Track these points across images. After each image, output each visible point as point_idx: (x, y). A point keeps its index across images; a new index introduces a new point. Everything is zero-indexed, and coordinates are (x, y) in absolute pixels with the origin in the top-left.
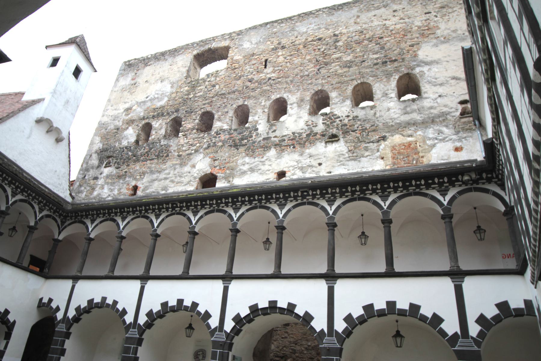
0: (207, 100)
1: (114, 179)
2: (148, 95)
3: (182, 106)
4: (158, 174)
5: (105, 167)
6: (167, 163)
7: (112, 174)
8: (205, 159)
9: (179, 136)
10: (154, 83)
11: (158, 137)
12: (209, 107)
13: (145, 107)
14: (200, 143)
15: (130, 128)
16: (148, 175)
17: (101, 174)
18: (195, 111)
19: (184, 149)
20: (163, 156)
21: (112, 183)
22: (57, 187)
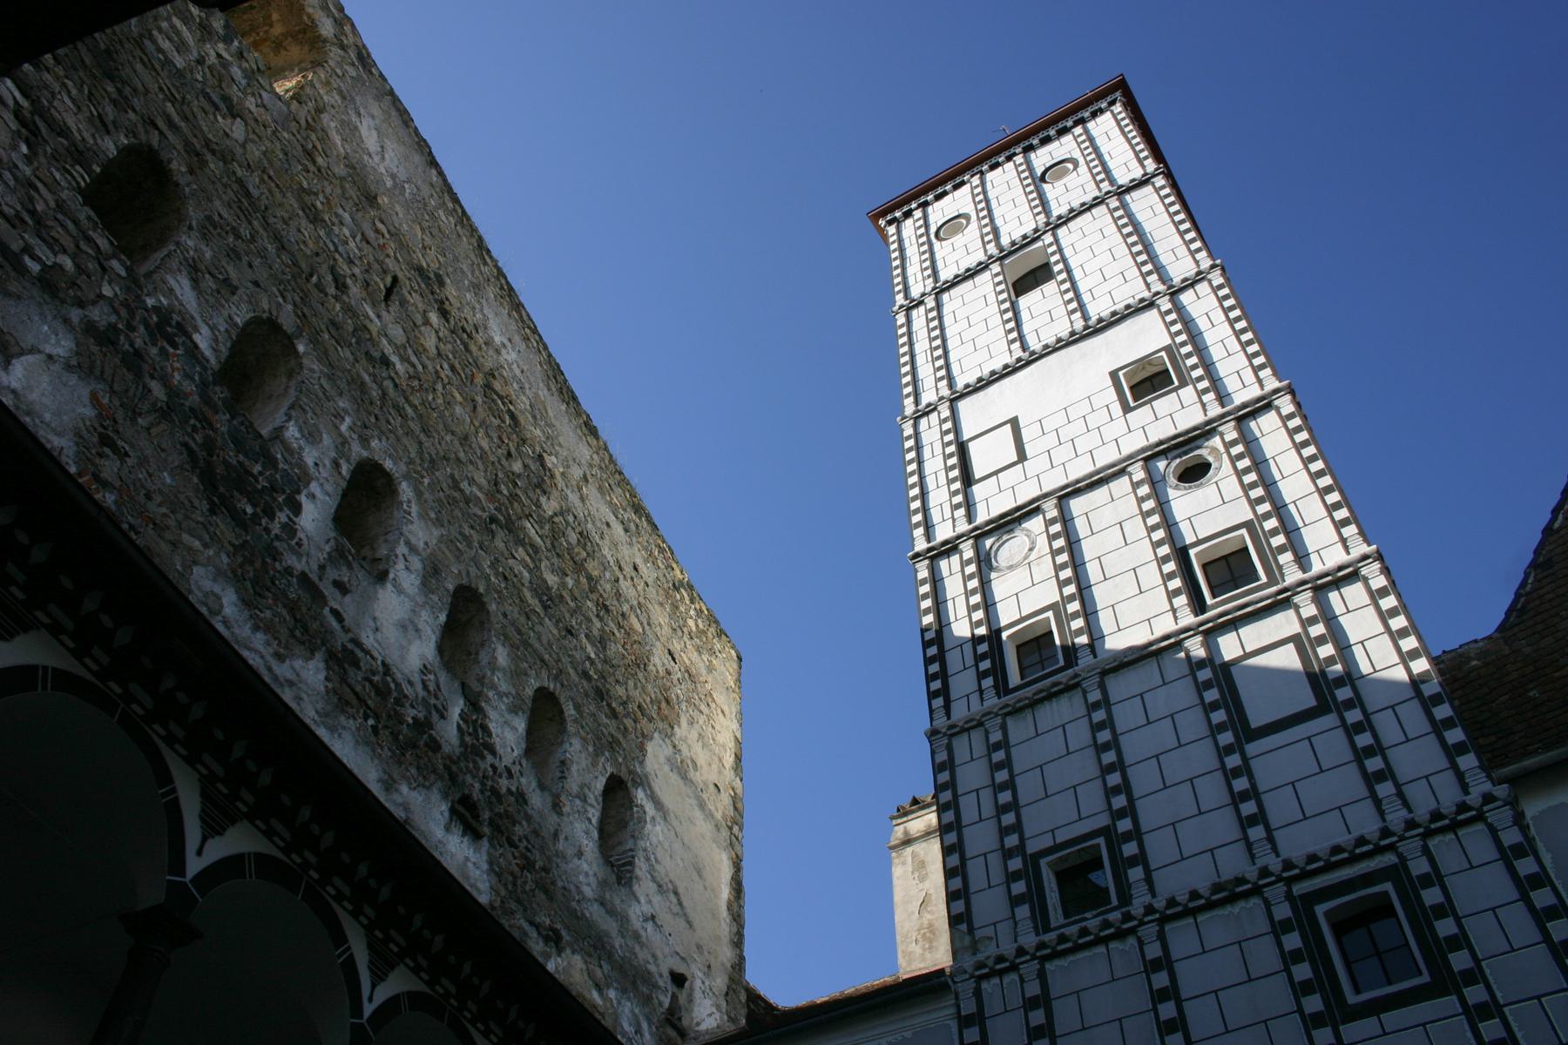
0: (186, 119)
8: (73, 380)
12: (183, 169)
18: (127, 91)
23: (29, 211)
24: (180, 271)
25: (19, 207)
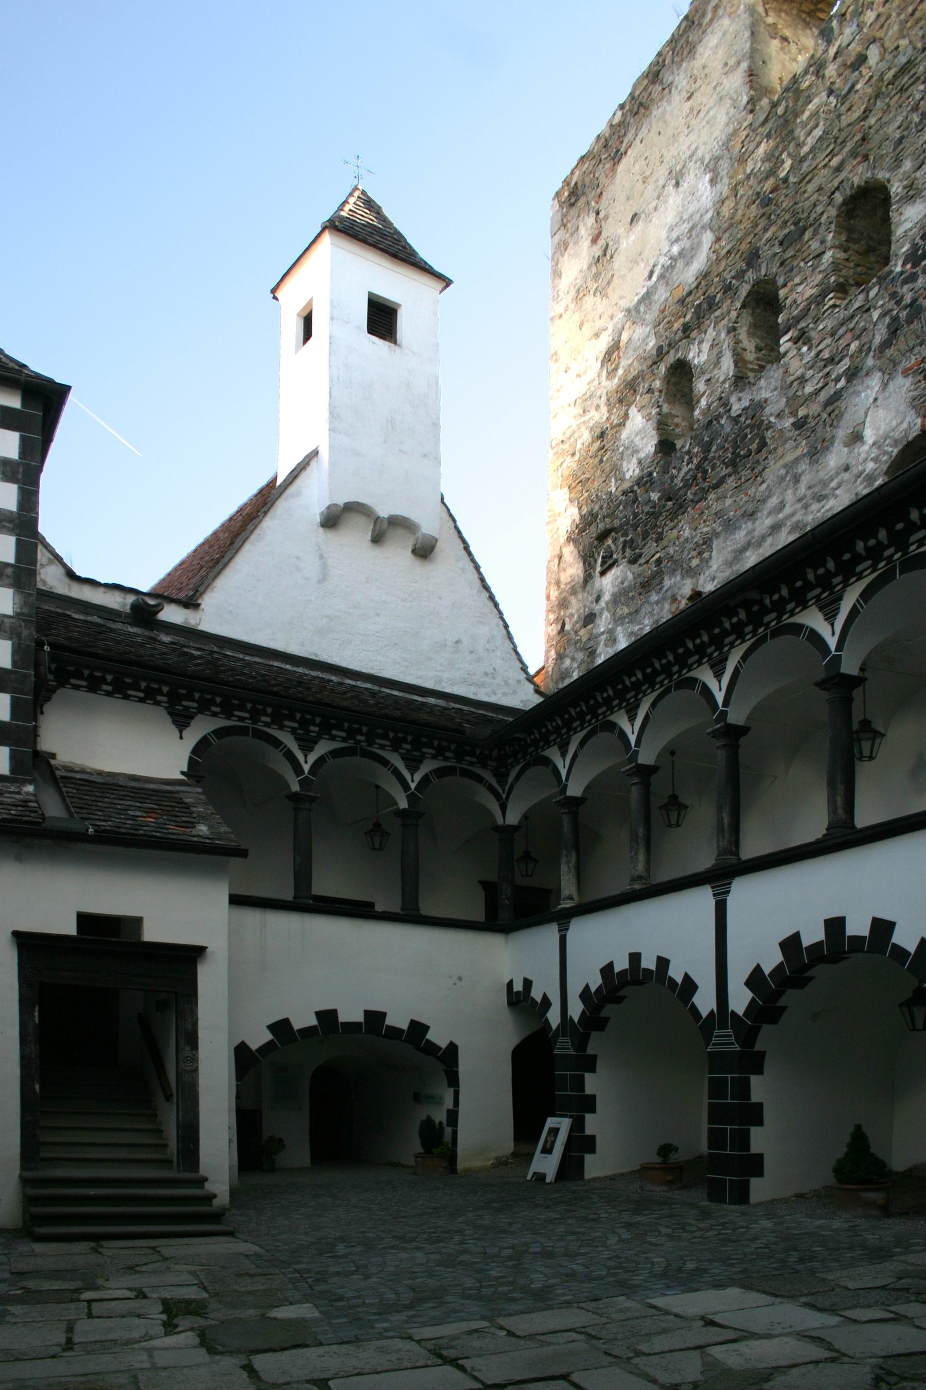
1: (633, 598)
2: (651, 263)
3: (765, 230)
4: (750, 524)
5: (603, 573)
6: (766, 474)
7: (626, 584)
8: (891, 385)
9: (782, 349)
10: (656, 209)
11: (718, 393)
12: (860, 169)
13: (656, 308)
14: (858, 337)
15: (633, 411)
16: (721, 539)
17: (598, 599)
19: (809, 389)
20: (748, 455)
21: (630, 614)
22: (483, 685)
23: (825, 366)
24: (901, 214)
25: (821, 374)
